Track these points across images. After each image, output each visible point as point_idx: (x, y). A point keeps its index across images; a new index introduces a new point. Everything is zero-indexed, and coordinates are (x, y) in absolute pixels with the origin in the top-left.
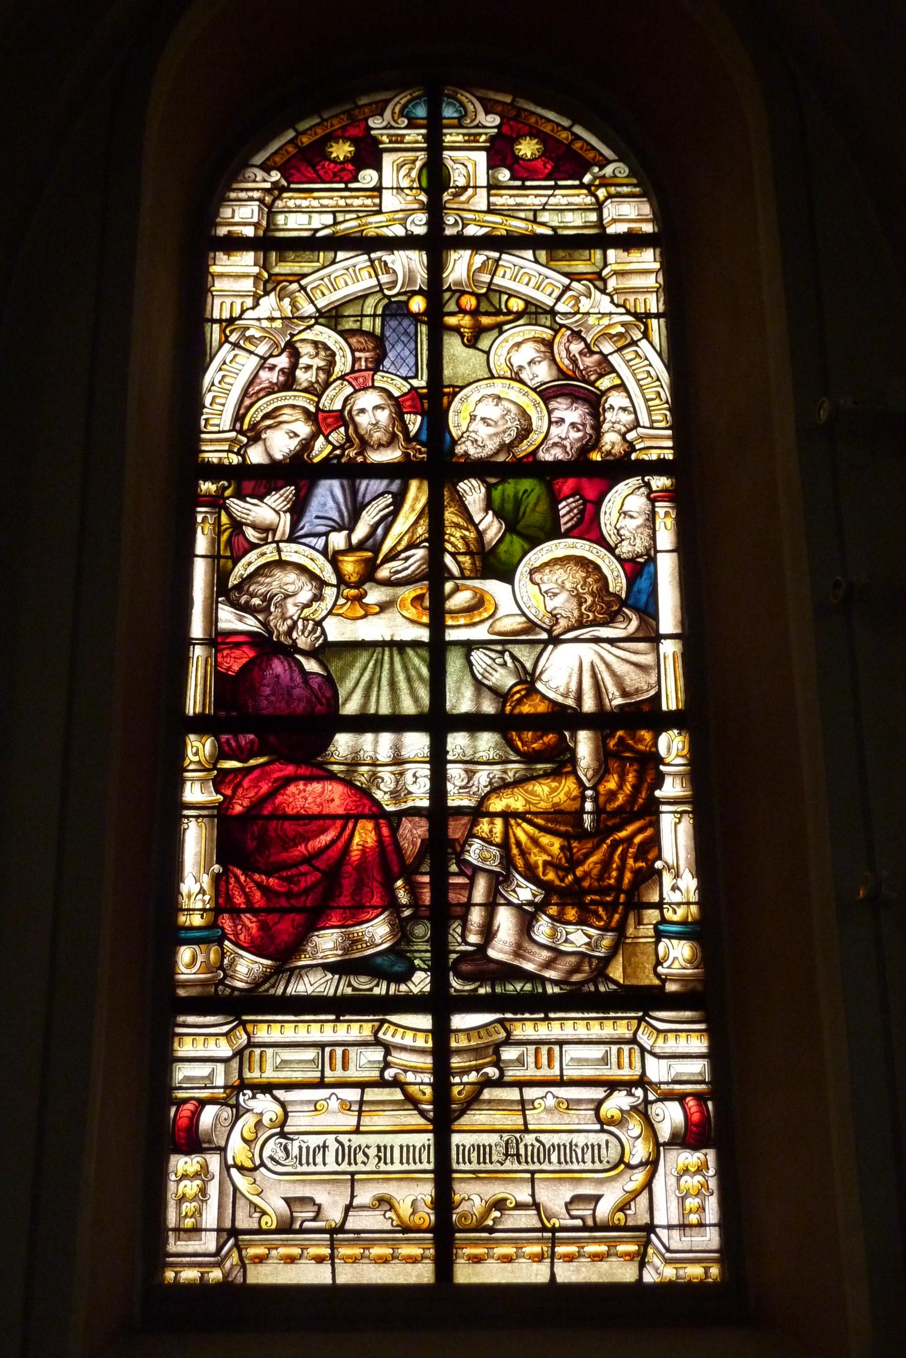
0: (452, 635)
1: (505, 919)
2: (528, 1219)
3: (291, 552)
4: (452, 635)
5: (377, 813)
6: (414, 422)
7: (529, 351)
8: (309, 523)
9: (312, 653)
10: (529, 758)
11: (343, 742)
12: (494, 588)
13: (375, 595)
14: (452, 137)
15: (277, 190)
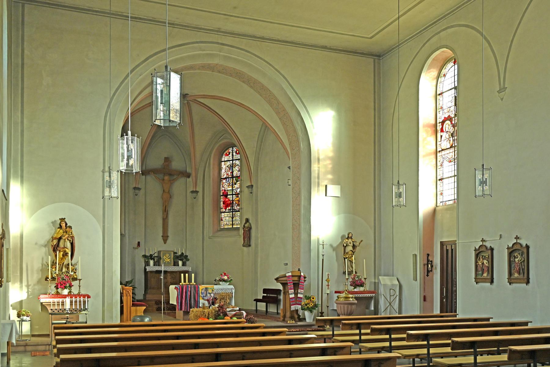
0: (233, 189)
1: (235, 207)
2: (236, 224)
3: (226, 184)
4: (233, 189)
5: (230, 201)
6: (232, 174)
7: (237, 168)
8: (227, 182)
9: (227, 191)
10: (237, 197)
11: (228, 196)
12: (235, 185)
13: (230, 186)
14: (234, 151)
15: (225, 157)
